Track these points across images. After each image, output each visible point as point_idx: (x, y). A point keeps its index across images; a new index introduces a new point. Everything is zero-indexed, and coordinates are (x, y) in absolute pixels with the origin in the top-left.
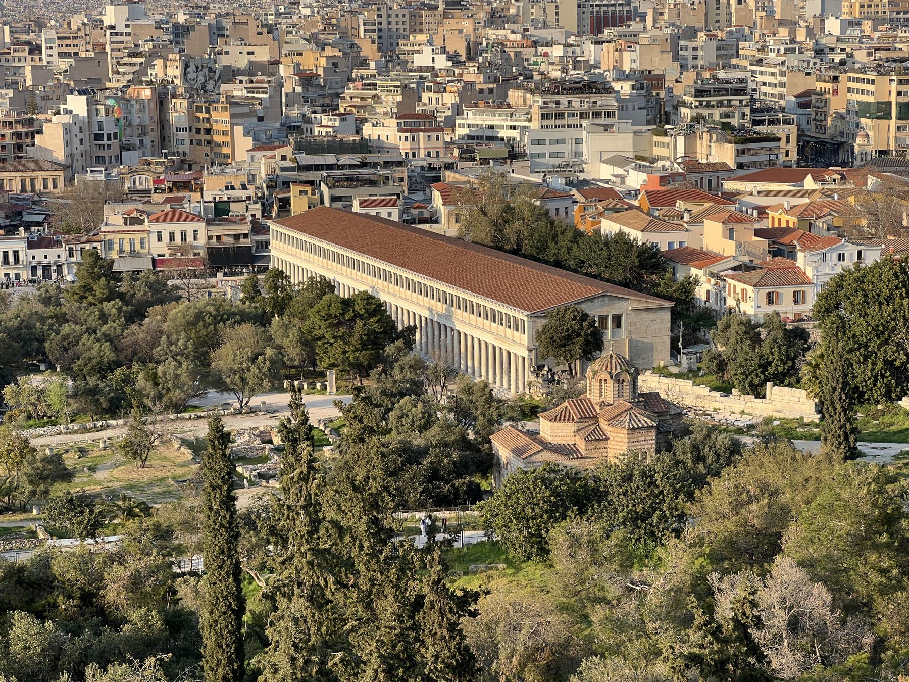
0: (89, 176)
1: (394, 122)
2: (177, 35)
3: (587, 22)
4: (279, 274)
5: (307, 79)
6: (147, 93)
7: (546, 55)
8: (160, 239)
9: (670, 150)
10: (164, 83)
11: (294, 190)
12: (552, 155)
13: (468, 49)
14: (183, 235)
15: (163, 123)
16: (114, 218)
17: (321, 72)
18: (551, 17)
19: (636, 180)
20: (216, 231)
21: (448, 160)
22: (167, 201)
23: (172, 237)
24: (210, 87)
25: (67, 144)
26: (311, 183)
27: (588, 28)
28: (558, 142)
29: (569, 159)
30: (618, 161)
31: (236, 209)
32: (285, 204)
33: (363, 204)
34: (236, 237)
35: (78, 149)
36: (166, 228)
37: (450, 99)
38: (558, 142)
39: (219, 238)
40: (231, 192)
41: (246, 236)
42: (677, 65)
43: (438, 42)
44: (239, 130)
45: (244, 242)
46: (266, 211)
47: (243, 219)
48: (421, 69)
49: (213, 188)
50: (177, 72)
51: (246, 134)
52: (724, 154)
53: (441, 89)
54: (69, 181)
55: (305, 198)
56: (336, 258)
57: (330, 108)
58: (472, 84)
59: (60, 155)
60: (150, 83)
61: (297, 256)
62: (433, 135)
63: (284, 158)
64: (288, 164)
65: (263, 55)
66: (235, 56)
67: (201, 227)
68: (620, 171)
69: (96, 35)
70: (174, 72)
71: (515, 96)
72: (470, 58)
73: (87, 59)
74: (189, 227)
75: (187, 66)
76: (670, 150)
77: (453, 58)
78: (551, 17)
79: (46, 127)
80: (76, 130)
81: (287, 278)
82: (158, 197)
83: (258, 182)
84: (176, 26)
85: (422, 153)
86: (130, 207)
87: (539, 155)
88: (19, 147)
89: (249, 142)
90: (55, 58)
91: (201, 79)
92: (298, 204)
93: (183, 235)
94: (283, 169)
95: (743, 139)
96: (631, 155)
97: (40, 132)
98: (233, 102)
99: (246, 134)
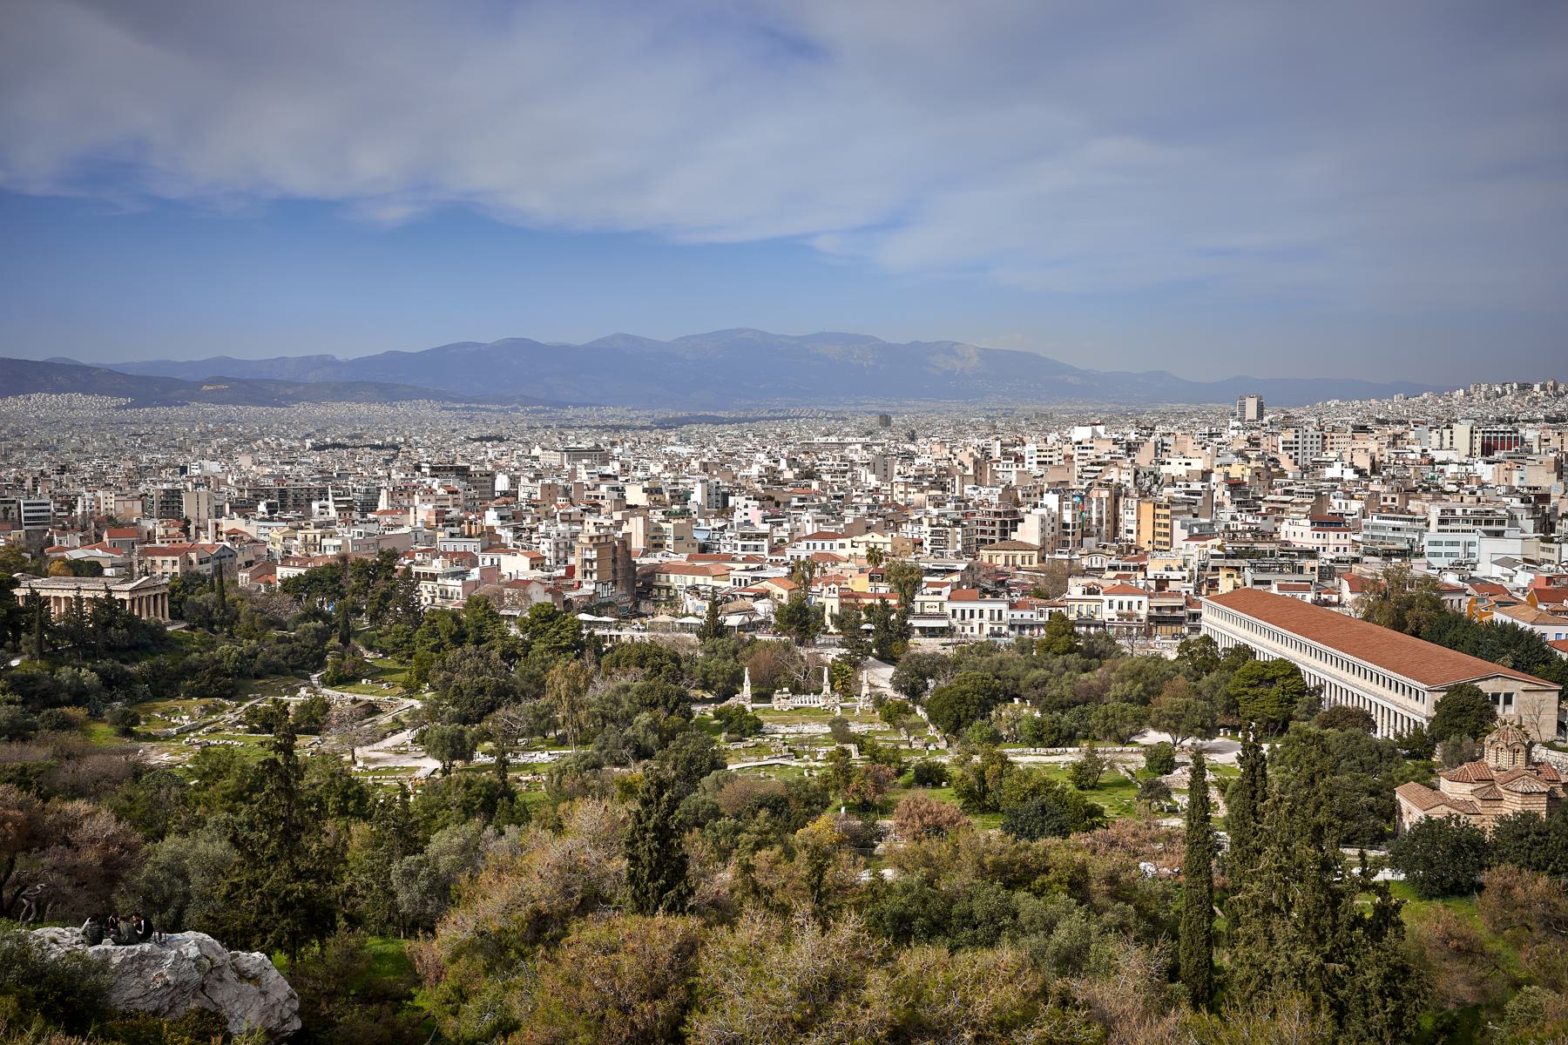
0: (1057, 556)
1: (1308, 522)
2: (1129, 450)
3: (1478, 445)
4: (1208, 640)
5: (1235, 486)
6: (1105, 494)
7: (1442, 471)
8: (1111, 606)
10: (1119, 486)
11: (1223, 574)
12: (1447, 555)
13: (1373, 464)
14: (1130, 604)
15: (1116, 519)
16: (1075, 588)
17: (1246, 479)
18: (1446, 443)
19: (1523, 579)
20: (1157, 602)
21: (1355, 555)
22: (1117, 577)
23: (1121, 605)
24: (1154, 489)
25: (1042, 530)
26: (1237, 569)
27: (1479, 450)
28: (1453, 544)
30: (1507, 562)
31: (1173, 586)
32: (1214, 584)
33: (1280, 588)
34: (1173, 608)
35: (1049, 534)
36: (1117, 599)
37: (1355, 506)
38: (1453, 544)
39: (1159, 609)
40: (1168, 573)
41: (1181, 608)
42: (1561, 484)
43: (1347, 461)
44: (1177, 524)
45: (1179, 613)
46: (1198, 591)
47: (1178, 594)
48: (1332, 480)
49: (1155, 568)
50: (1130, 478)
51: (1183, 527)
54: (1042, 559)
55: (1231, 581)
56: (1262, 630)
57: (1254, 511)
58: (1378, 493)
59: (1035, 540)
60: (1107, 486)
61: (1224, 627)
62: (1342, 534)
63: (1213, 547)
64: (1216, 552)
65: (1198, 465)
66: (1175, 468)
67: (1145, 599)
68: (1509, 571)
69: (1067, 449)
70: (1126, 478)
71: (1413, 505)
72: (1374, 471)
73: (1059, 466)
74: (1135, 599)
75: (1137, 473)
77: (1359, 471)
78: (1446, 443)
79: (1027, 517)
80: (1049, 520)
81: (1216, 644)
82: (1112, 574)
83: (1191, 566)
84: (1129, 444)
85: (1331, 548)
86: (1088, 580)
87: (1435, 555)
88: (1004, 533)
89: (1185, 534)
90: (1034, 465)
91: (1148, 483)
92: (1225, 585)
93: (1130, 604)
94: (1213, 556)
96: (1519, 558)
97: (1022, 521)
99: (1183, 527)
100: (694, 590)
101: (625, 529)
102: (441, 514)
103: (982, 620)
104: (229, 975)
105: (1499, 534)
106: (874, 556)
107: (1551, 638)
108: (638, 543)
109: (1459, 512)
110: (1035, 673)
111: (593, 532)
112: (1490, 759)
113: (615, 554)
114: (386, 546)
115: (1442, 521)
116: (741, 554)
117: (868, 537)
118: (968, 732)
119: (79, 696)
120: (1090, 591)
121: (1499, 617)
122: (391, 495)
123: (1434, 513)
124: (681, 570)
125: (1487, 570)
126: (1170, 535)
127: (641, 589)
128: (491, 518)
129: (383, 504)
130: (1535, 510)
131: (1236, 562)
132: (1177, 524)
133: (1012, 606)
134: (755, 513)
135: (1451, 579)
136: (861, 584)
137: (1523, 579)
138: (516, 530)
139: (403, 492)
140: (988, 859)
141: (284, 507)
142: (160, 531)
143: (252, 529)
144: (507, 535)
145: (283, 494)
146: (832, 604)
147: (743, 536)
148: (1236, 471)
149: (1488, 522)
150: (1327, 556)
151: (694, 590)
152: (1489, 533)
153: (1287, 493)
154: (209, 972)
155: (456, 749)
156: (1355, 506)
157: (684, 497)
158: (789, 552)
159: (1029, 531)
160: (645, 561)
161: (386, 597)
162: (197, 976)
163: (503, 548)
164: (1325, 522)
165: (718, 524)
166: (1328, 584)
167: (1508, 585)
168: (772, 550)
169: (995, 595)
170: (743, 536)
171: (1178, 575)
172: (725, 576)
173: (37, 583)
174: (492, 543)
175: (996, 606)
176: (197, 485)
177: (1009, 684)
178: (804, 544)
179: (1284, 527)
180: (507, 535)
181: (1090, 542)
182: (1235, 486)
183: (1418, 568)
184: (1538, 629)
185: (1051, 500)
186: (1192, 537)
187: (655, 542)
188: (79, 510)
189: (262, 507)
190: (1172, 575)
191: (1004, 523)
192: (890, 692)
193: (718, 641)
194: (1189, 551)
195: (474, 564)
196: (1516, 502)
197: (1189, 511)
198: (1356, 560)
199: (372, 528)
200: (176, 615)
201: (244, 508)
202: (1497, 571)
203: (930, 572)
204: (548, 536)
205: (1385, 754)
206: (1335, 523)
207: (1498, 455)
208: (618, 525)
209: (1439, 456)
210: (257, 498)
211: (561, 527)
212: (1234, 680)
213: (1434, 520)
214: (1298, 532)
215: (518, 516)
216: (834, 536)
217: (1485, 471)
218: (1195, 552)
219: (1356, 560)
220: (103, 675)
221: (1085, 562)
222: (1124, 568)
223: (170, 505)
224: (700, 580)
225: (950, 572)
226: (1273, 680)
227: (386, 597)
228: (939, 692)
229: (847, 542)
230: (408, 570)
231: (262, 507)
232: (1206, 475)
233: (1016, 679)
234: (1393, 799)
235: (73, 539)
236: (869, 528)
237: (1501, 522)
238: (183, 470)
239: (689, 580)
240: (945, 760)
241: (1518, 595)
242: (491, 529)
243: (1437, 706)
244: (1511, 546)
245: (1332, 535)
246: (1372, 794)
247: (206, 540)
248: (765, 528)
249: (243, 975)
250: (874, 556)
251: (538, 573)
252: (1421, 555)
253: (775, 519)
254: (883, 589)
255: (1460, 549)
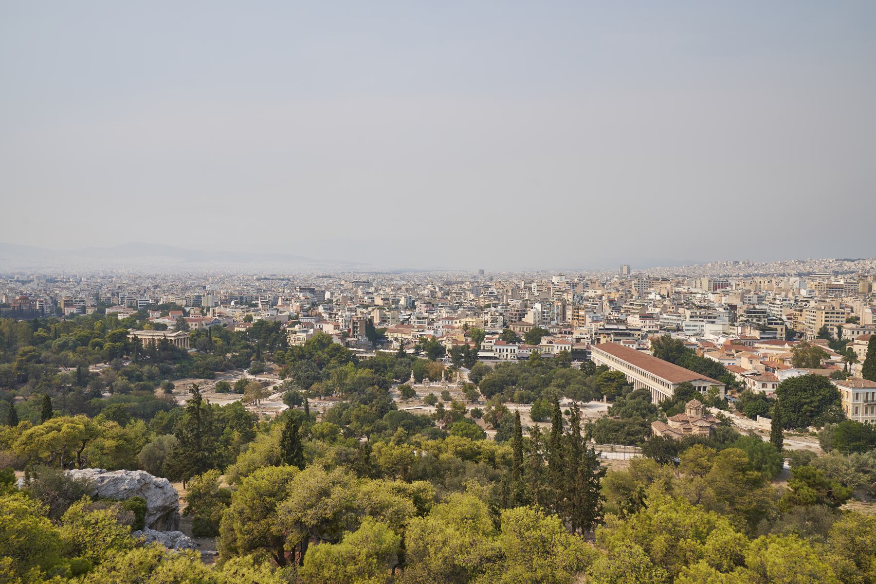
5: (611, 302)
9: (737, 332)
15: (564, 313)
29: (699, 332)
30: (716, 333)
37: (658, 310)
52: (756, 334)
53: (655, 306)
57: (618, 311)
71: (681, 310)
76: (737, 332)
82: (560, 336)
88: (520, 318)
89: (590, 320)
95: (763, 329)
98: (586, 307)
100: (396, 339)
101: (372, 314)
102: (301, 308)
103: (509, 353)
104: (152, 486)
105: (713, 322)
106: (466, 327)
107: (726, 364)
108: (376, 321)
109: (698, 313)
110: (524, 374)
111: (360, 316)
112: (687, 412)
113: (369, 324)
114: (277, 320)
115: (691, 317)
116: (416, 325)
117: (466, 319)
118: (494, 397)
119: (151, 377)
120: (551, 342)
121: (707, 356)
122: (283, 299)
123: (688, 313)
124: (392, 331)
125: (709, 337)
126: (585, 320)
127: (376, 337)
128: (321, 309)
129: (280, 303)
130: (730, 313)
131: (609, 332)
132: (587, 316)
133: (519, 348)
134: (424, 309)
135: (693, 340)
136: (461, 338)
137: (722, 340)
138: (330, 314)
139: (286, 300)
140: (459, 448)
141: (241, 304)
142: (192, 312)
143: (228, 311)
144: (326, 316)
145: (242, 298)
146: (449, 346)
147: (418, 318)
148: (612, 296)
149: (710, 318)
150: (647, 329)
151: (396, 339)
152: (709, 322)
153: (631, 304)
154: (144, 485)
155: (292, 400)
156: (658, 310)
157: (396, 302)
158: (435, 324)
159: (529, 318)
160: (380, 327)
161: (275, 340)
162: (138, 486)
163: (325, 321)
164: (644, 317)
165: (409, 313)
166: (644, 341)
167: (715, 343)
168: (429, 324)
169: (514, 343)
170: (418, 318)
171: (585, 336)
172: (409, 334)
173: (137, 333)
174: (320, 319)
175: (513, 348)
176: (208, 294)
177: (514, 378)
178: (441, 322)
179: (629, 318)
180: (326, 316)
181: (553, 323)
182: (611, 302)
183: (680, 336)
184: (722, 361)
185: (538, 306)
186: (593, 322)
187: (384, 320)
188: (161, 303)
189: (233, 303)
190: (582, 336)
191: (520, 315)
192: (468, 381)
193: (402, 359)
194: (591, 326)
195: (312, 327)
196: (722, 310)
197: (592, 311)
198: (656, 332)
199: (274, 312)
200: (193, 346)
201: (226, 303)
202: (712, 337)
203: (488, 334)
204: (342, 316)
205: (652, 410)
206: (650, 317)
207: (718, 291)
208: (369, 313)
209: (692, 290)
210: (231, 299)
211: (347, 313)
212: (599, 378)
213: (688, 317)
214: (634, 321)
215: (331, 309)
216: (454, 319)
217: (712, 297)
218: (594, 327)
219: (656, 332)
220: (161, 369)
221: (551, 331)
222: (565, 333)
223: (197, 302)
224: (399, 335)
225: (497, 333)
226: (613, 380)
227: (275, 340)
228: (485, 381)
229: (458, 321)
230: (285, 330)
231: (233, 303)
232: (601, 297)
233: (517, 376)
234: (650, 428)
235: (158, 314)
236: (467, 316)
237: (715, 318)
238: (204, 287)
239: (395, 335)
240: (482, 408)
241: (719, 347)
242: (320, 314)
243: (675, 391)
244: (718, 327)
245: (648, 322)
246: (642, 425)
247: (209, 315)
248: (426, 315)
249: (158, 486)
250: (466, 327)
251: (337, 331)
252: (682, 330)
253: (430, 312)
254: (469, 340)
255: (697, 328)
